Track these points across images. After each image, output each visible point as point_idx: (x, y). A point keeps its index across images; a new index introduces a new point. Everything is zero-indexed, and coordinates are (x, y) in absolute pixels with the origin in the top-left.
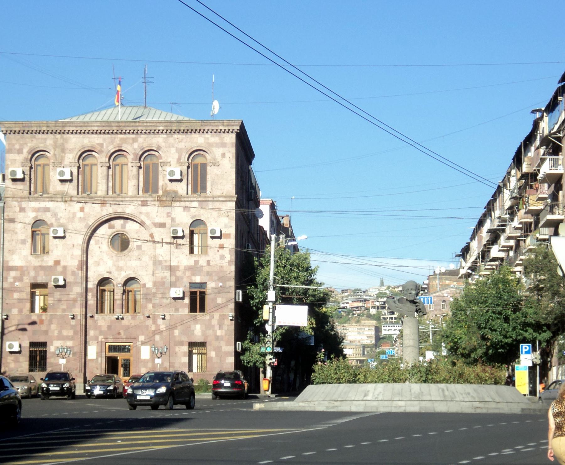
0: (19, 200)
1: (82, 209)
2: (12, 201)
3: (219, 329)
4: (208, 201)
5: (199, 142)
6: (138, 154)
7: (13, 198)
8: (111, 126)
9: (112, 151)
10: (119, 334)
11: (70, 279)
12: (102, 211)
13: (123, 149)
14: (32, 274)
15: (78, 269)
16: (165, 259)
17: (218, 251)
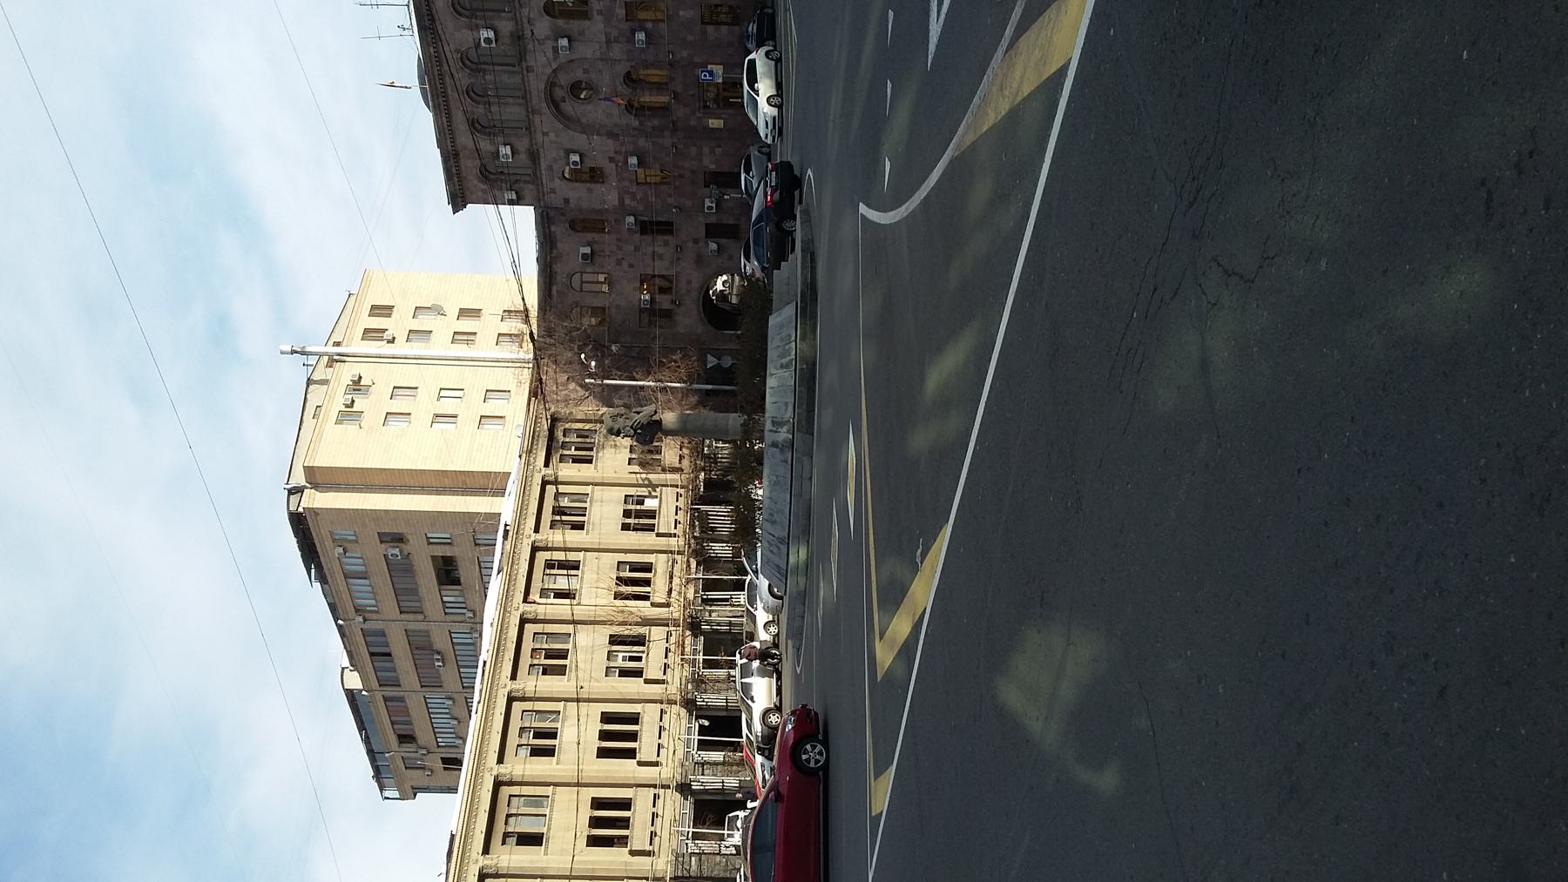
0: (541, 194)
1: (545, 134)
2: (544, 200)
6: (469, 74)
7: (540, 200)
8: (439, 105)
10: (693, 95)
11: (631, 148)
14: (626, 183)
15: (618, 140)
16: (598, 48)
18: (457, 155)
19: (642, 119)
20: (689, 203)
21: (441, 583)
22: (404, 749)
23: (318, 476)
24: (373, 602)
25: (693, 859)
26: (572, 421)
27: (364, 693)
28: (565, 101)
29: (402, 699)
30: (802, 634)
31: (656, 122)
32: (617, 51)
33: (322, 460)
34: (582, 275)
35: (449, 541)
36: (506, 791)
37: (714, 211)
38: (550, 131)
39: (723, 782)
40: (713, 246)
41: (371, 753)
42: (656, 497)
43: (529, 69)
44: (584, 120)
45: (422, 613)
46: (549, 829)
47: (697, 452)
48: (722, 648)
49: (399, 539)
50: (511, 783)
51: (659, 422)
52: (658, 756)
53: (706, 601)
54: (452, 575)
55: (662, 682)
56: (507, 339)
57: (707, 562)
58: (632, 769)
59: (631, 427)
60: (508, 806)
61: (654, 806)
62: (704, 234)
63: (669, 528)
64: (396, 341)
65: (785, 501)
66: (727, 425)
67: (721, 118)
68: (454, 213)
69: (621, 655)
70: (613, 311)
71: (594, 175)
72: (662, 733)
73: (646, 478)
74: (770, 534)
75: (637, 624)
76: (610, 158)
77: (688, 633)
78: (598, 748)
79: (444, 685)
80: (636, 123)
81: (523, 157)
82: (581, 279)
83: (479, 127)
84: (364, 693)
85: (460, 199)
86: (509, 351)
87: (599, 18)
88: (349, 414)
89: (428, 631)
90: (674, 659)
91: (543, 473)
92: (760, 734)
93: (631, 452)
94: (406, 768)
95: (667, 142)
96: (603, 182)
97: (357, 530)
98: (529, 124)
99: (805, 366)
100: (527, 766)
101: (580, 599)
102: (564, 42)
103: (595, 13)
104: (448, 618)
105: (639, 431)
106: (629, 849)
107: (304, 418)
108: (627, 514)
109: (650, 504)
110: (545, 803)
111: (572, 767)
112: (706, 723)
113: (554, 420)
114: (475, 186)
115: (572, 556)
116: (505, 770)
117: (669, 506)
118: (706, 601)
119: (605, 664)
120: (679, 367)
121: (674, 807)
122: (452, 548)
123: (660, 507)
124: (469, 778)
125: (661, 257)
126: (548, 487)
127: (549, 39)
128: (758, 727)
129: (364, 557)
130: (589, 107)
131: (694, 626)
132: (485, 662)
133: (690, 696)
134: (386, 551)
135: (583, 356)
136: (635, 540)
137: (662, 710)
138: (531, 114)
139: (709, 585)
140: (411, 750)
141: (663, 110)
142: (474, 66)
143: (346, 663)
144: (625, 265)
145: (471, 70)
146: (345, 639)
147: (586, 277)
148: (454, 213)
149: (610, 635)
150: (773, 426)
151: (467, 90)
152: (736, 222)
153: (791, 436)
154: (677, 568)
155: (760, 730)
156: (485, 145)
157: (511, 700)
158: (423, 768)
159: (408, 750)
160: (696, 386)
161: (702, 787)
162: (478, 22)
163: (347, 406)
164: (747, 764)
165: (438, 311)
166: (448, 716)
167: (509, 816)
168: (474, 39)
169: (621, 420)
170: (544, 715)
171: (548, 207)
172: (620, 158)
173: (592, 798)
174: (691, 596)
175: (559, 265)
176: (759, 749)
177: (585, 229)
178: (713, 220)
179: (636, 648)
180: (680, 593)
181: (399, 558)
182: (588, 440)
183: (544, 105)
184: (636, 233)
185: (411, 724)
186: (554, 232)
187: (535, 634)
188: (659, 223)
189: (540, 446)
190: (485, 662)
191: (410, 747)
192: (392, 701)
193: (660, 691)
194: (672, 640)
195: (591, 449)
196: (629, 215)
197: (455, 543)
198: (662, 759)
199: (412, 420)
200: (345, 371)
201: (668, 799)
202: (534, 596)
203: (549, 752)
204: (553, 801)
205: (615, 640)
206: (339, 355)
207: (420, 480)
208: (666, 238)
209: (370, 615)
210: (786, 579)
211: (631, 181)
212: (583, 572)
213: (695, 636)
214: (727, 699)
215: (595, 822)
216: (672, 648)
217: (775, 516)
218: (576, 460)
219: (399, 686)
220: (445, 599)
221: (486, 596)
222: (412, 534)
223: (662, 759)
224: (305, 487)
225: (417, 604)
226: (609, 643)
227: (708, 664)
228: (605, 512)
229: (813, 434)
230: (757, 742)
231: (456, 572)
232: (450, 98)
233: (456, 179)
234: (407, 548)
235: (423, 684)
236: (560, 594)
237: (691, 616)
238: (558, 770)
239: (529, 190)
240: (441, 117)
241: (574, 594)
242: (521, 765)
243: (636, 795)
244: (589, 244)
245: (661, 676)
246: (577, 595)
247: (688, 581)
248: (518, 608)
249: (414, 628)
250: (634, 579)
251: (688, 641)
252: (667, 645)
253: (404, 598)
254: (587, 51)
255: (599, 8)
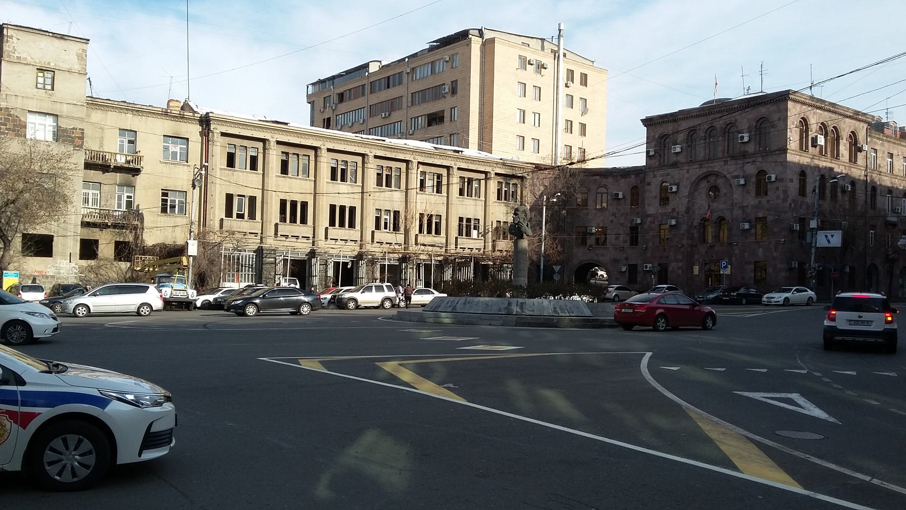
3: (776, 251)
4: (767, 155)
5: (763, 111)
7: (649, 169)
8: (704, 111)
9: (707, 128)
10: (712, 257)
11: (681, 220)
12: (700, 171)
13: (713, 125)
14: (660, 219)
17: (775, 192)
18: (675, 121)
19: (698, 227)
20: (649, 255)
21: (429, 115)
22: (335, 97)
23: (490, 45)
24: (418, 78)
25: (273, 259)
26: (522, 188)
27: (367, 74)
28: (707, 182)
29: (363, 95)
30: (400, 320)
31: (696, 235)
32: (738, 212)
33: (498, 48)
34: (605, 193)
35: (453, 120)
36: (312, 153)
37: (645, 269)
38: (688, 175)
39: (316, 276)
40: (624, 269)
41: (333, 78)
42: (478, 237)
43: (726, 162)
44: (696, 194)
45: (412, 105)
46: (290, 178)
47: (504, 260)
48: (392, 275)
49: (454, 91)
50: (316, 156)
51: (522, 237)
52: (331, 239)
53: (418, 266)
54: (433, 122)
55: (373, 241)
56: (568, 151)
57: (441, 266)
58: (324, 224)
59: (519, 222)
60: (304, 155)
61: (303, 237)
62: (631, 263)
63: (460, 244)
64: (567, 88)
65: (477, 310)
66: (521, 277)
67: (699, 273)
68: (641, 120)
69: (388, 217)
70: (585, 211)
71: (664, 200)
72: (344, 241)
73: (489, 231)
74: (458, 302)
75: (406, 226)
76: (675, 208)
77: (401, 256)
78: (336, 205)
79: (371, 118)
80: (695, 224)
81: (674, 159)
82: (604, 193)
83: (691, 133)
84: (367, 74)
85: (649, 123)
86: (561, 152)
87: (757, 201)
88: (525, 62)
89: (401, 109)
90: (386, 247)
91: (492, 172)
92: (343, 297)
93: (504, 222)
94: (325, 98)
95: (685, 242)
96: (660, 205)
97: (459, 68)
98: (694, 162)
99: (555, 321)
100: (326, 164)
101: (420, 194)
102: (742, 182)
103: (760, 200)
104: (409, 120)
105: (517, 226)
106: (279, 223)
107: (522, 37)
108: (469, 220)
109: (474, 233)
110: (305, 176)
111: (325, 191)
112: (349, 266)
113: (522, 178)
114: (657, 131)
115: (444, 188)
116: (324, 153)
117: (473, 244)
118: (418, 266)
119: (383, 209)
120: (553, 249)
121: (302, 248)
122: (449, 121)
123: (473, 239)
124: (319, 132)
125: (617, 238)
126: (484, 175)
127: (744, 173)
128: (347, 295)
129: (444, 72)
130: (704, 196)
131: (404, 259)
132: (384, 141)
133: (365, 257)
134: (447, 85)
135: (559, 194)
136: (454, 225)
137: (357, 241)
138: (699, 163)
139: (428, 268)
140: (335, 100)
141: (704, 240)
142: (727, 130)
143: (384, 63)
144: (612, 218)
145: (725, 129)
146: (397, 62)
147: (605, 196)
148: (641, 120)
149: (399, 211)
150: (520, 303)
151: (713, 126)
152: (638, 282)
153: (514, 313)
154: (438, 249)
155: (345, 297)
156: (681, 137)
157: (363, 156)
158: (325, 107)
159: (335, 98)
160: (542, 259)
161: (313, 264)
162: (753, 132)
163: (529, 61)
164: (326, 289)
165: (585, 111)
166: (354, 121)
167: (298, 155)
168: (743, 130)
169: (523, 215)
170: (354, 175)
171: (645, 173)
172: (675, 214)
173: (307, 202)
174: (422, 257)
175: (611, 180)
176: (335, 296)
177: (632, 195)
178: (639, 269)
179: (392, 226)
180: (423, 251)
181: (443, 92)
182: (510, 198)
183: (705, 170)
184: (631, 224)
185: (350, 99)
186: (631, 177)
187: (400, 169)
188: (637, 237)
189: (507, 170)
190: (384, 141)
191: (336, 99)
192: (362, 89)
193: (367, 240)
194: (397, 247)
195: (505, 200)
196: (641, 220)
197: (451, 123)
198: (329, 241)
199: (521, 98)
200: (549, 60)
201: (306, 245)
202: (422, 168)
203: (333, 177)
204: (306, 180)
205: (396, 213)
206: (559, 56)
207: (488, 103)
208: (629, 242)
209: (411, 76)
210: (432, 311)
211: (661, 221)
212: (435, 195)
213: (399, 260)
214: (363, 278)
215: (294, 204)
216: (392, 247)
217: (468, 305)
218: (499, 191)
219: (371, 93)
220: (420, 118)
221: (421, 141)
222: (456, 99)
223: (329, 241)
224: (483, 39)
225: (417, 103)
226: (395, 211)
227: (383, 267)
228: (470, 208)
229: (515, 326)
230: (339, 295)
231: (435, 124)
232: (707, 117)
233: (661, 121)
234: (449, 96)
235: (372, 106)
236: (422, 183)
237: (410, 257)
238: (324, 183)
239: (655, 162)
240: (697, 112)
241: (422, 191)
242: (326, 162)
243: (309, 226)
244: (624, 197)
245: (376, 240)
246: (422, 192)
247: (430, 255)
248: (415, 159)
249: (403, 101)
250: (431, 225)
251: (396, 256)
252: (394, 244)
253: (421, 95)
254: (737, 195)
255: (762, 202)
